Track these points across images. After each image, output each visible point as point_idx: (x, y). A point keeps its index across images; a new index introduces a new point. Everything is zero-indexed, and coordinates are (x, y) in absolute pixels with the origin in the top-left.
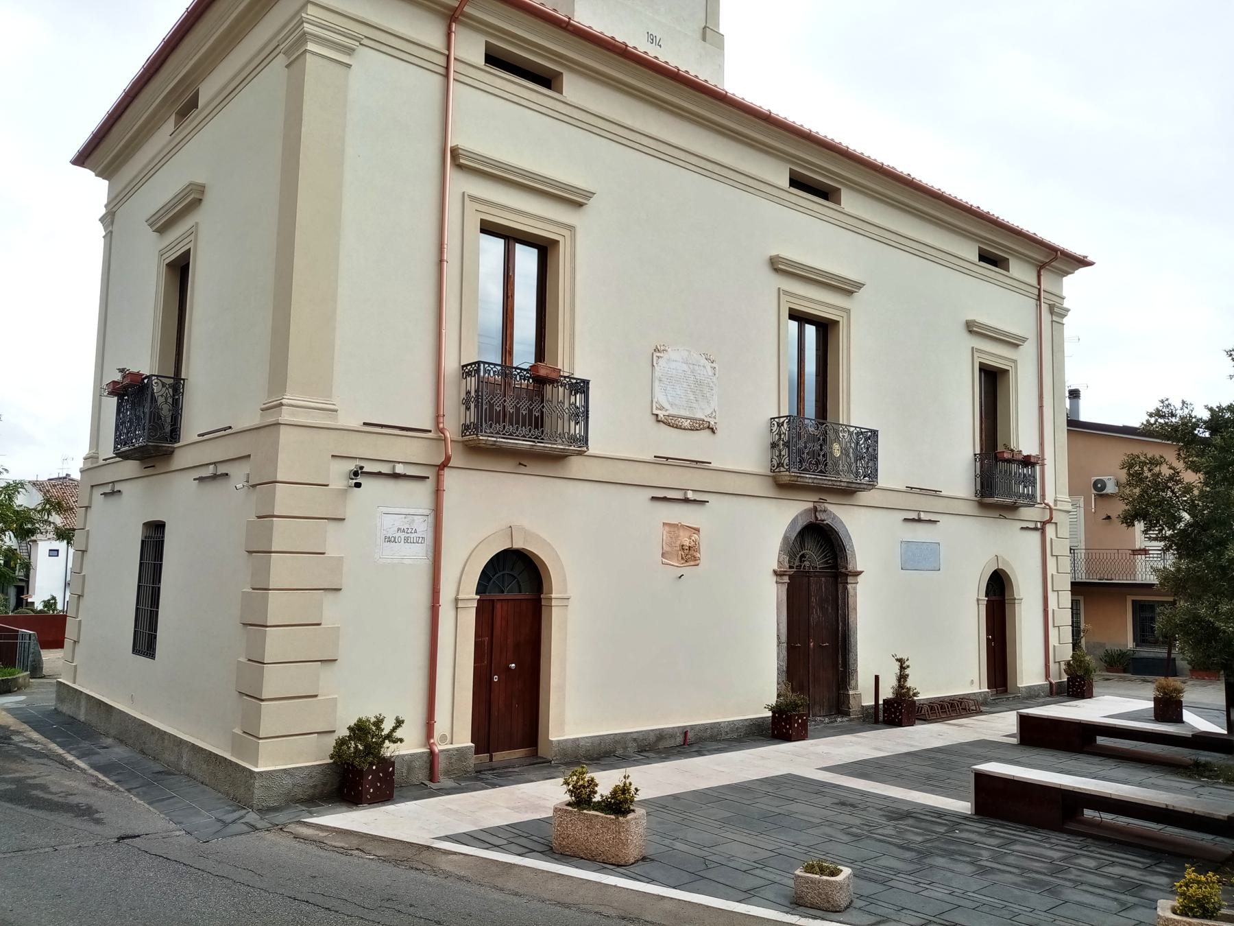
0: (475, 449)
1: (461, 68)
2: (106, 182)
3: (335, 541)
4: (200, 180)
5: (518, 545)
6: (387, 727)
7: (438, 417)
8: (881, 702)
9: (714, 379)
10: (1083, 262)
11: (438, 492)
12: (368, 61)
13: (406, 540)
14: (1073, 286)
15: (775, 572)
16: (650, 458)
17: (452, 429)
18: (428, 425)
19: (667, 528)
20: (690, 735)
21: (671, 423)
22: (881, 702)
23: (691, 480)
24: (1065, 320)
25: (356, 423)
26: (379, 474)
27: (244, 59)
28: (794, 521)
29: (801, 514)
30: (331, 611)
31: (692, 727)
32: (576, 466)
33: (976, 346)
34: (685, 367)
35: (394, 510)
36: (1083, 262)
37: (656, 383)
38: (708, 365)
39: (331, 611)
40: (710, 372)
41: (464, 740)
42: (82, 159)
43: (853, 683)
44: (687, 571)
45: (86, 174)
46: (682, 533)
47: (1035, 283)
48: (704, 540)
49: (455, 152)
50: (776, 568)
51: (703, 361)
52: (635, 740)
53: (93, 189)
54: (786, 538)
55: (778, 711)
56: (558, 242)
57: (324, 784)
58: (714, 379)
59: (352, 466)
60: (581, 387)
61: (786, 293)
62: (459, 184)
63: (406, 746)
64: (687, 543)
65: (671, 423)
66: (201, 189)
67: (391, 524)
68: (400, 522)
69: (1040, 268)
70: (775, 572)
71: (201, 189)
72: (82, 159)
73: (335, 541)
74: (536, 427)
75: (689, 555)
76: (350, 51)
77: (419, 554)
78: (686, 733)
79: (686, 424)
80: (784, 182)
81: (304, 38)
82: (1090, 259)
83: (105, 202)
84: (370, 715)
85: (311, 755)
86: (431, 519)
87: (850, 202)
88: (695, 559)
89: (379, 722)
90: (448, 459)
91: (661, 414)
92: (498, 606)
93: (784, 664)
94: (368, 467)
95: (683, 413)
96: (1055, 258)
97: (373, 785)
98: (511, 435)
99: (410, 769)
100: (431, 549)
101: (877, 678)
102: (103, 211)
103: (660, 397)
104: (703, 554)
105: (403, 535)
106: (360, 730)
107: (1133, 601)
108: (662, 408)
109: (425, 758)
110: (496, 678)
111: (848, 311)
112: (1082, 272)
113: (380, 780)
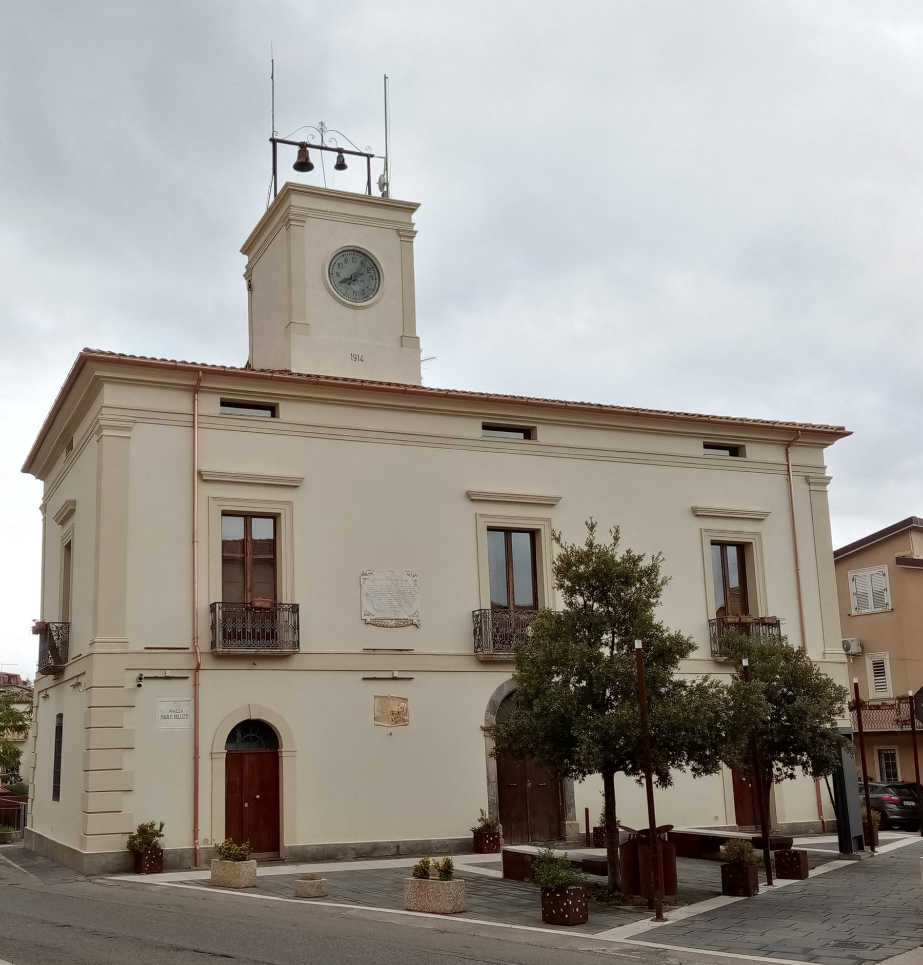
0: (219, 657)
1: (202, 419)
2: (42, 482)
3: (129, 719)
4: (73, 498)
5: (255, 716)
6: (157, 827)
7: (195, 638)
8: (591, 831)
9: (416, 589)
10: (839, 433)
11: (196, 685)
12: (142, 432)
13: (176, 717)
14: (833, 456)
15: (482, 727)
16: (361, 651)
17: (204, 644)
18: (187, 643)
19: (378, 699)
20: (401, 848)
21: (378, 624)
22: (591, 831)
23: (397, 664)
24: (828, 487)
25: (140, 648)
26: (156, 678)
27: (85, 429)
28: (500, 688)
29: (506, 683)
30: (128, 761)
31: (404, 843)
32: (297, 662)
33: (703, 527)
34: (389, 583)
35: (168, 699)
36: (839, 433)
37: (364, 598)
38: (410, 579)
39: (128, 761)
40: (411, 583)
41: (220, 838)
42: (27, 468)
43: (570, 815)
44: (397, 730)
45: (30, 477)
46: (391, 702)
47: (784, 461)
48: (411, 706)
49: (199, 473)
50: (483, 725)
51: (405, 577)
52: (353, 849)
53: (35, 487)
54: (492, 702)
55: (478, 833)
56: (280, 514)
57: (126, 864)
58: (416, 589)
59: (136, 674)
60: (295, 609)
61: (482, 516)
62: (205, 491)
63: (173, 840)
64: (396, 709)
65: (378, 624)
66: (74, 503)
67: (164, 707)
68: (171, 706)
69: (788, 445)
70: (482, 727)
71: (74, 503)
72: (27, 468)
73: (129, 719)
74: (268, 639)
75: (399, 718)
76: (129, 429)
77: (186, 725)
78: (398, 846)
79: (392, 623)
80: (478, 432)
81: (101, 428)
82: (847, 430)
83: (42, 495)
84: (147, 822)
85: (117, 845)
86: (192, 703)
87: (544, 434)
88: (404, 721)
89: (152, 825)
90: (199, 665)
91: (368, 620)
92: (246, 757)
93: (496, 799)
94: (146, 674)
95: (388, 616)
96: (798, 437)
97: (149, 862)
98: (239, 646)
99: (181, 858)
100: (193, 722)
101: (587, 810)
102: (41, 502)
103: (367, 606)
104: (412, 716)
105: (173, 714)
106: (143, 830)
107: (879, 751)
108: (370, 614)
109: (192, 852)
110: (246, 805)
111: (549, 520)
112: (840, 442)
113: (153, 859)
